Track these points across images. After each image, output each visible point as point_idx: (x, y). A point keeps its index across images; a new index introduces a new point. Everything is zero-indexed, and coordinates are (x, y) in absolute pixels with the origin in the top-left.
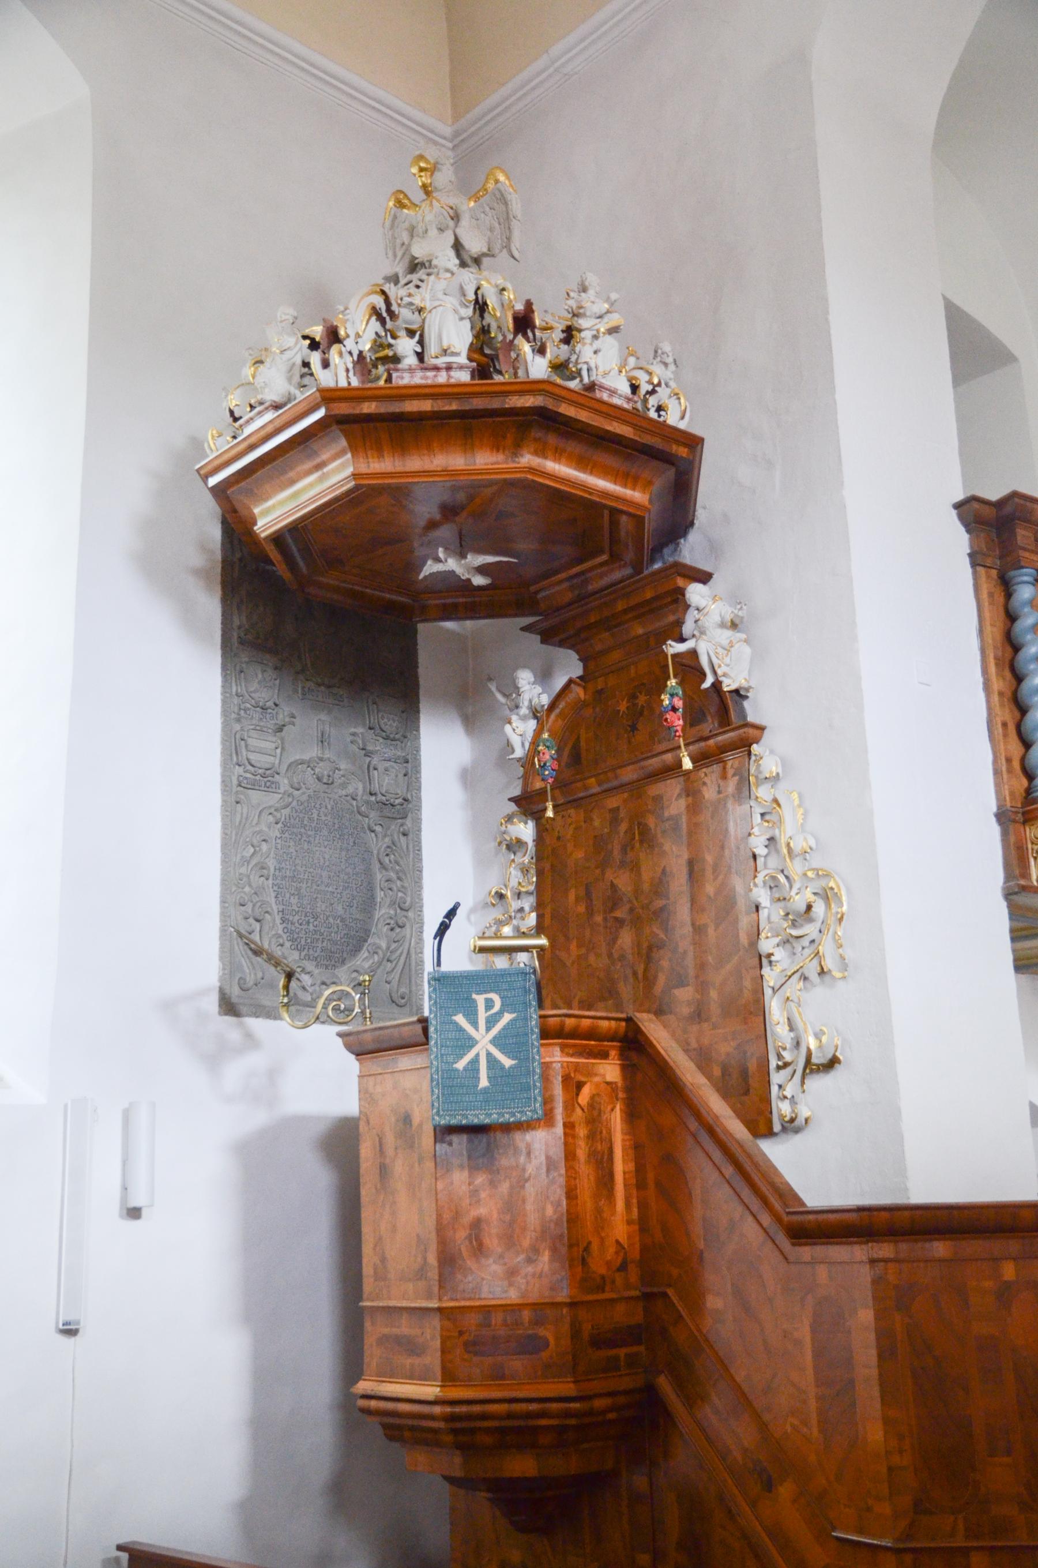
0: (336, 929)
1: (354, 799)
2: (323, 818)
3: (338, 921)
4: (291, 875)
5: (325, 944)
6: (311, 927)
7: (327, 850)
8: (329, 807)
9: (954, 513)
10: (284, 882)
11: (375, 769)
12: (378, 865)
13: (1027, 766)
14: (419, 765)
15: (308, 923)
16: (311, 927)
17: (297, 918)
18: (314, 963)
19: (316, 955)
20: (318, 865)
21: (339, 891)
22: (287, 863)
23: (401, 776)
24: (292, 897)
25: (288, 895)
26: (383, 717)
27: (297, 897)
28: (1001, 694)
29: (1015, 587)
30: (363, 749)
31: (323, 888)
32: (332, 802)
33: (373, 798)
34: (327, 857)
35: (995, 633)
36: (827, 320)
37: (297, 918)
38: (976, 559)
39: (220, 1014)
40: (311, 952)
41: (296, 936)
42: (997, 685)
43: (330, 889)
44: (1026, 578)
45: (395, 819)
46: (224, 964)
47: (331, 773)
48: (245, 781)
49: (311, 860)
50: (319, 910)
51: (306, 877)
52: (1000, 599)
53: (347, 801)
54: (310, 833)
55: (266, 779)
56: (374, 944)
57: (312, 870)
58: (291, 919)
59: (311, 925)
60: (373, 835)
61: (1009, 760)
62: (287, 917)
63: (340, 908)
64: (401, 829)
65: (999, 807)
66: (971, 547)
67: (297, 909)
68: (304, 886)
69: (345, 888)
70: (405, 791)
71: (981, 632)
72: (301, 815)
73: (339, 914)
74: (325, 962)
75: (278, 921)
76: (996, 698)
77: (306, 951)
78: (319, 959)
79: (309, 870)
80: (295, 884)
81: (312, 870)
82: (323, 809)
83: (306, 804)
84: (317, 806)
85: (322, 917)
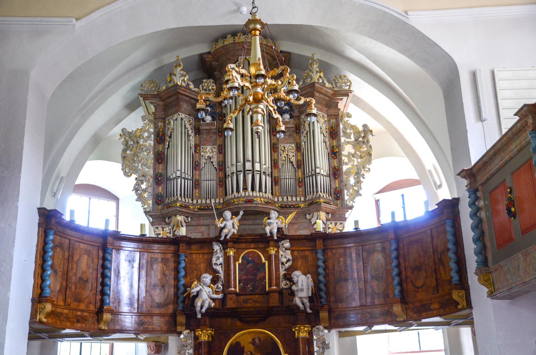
9: (37, 210)
13: (42, 286)
28: (39, 265)
29: (49, 235)
35: (40, 247)
36: (22, 152)
38: (40, 225)
42: (38, 262)
44: (51, 233)
52: (43, 237)
61: (38, 284)
65: (33, 298)
66: (39, 220)
71: (37, 246)
76: (38, 265)
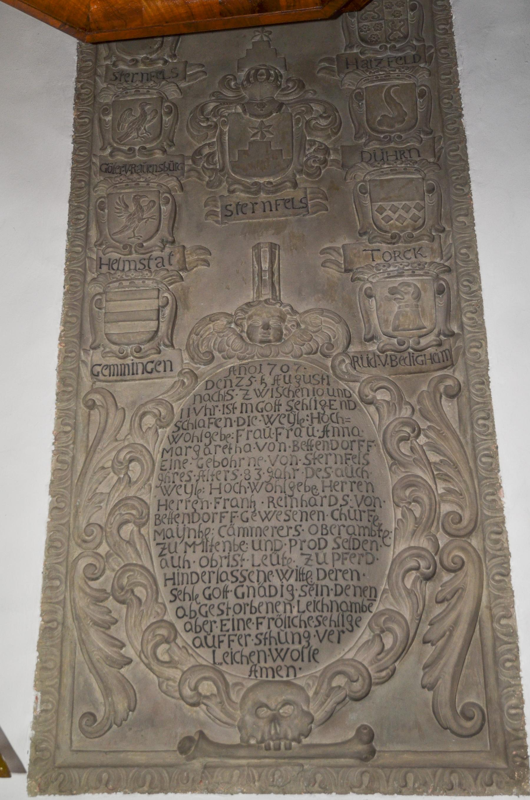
0: (287, 596)
1: (326, 356)
2: (255, 400)
3: (292, 581)
4: (190, 510)
5: (263, 629)
6: (232, 599)
7: (265, 453)
8: (269, 380)
10: (174, 526)
11: (370, 297)
12: (387, 460)
14: (477, 268)
15: (225, 592)
16: (232, 599)
17: (199, 588)
18: (246, 668)
19: (246, 651)
20: (245, 483)
21: (292, 523)
22: (181, 491)
23: (428, 297)
24: (190, 550)
25: (181, 548)
26: (381, 210)
27: (199, 549)
30: (347, 271)
31: (257, 523)
32: (277, 371)
33: (373, 348)
34: (265, 466)
37: (199, 588)
39: (31, 792)
40: (235, 646)
41: (201, 620)
43: (274, 522)
45: (428, 371)
46: (44, 693)
47: (272, 322)
48: (106, 372)
49: (230, 476)
50: (247, 565)
51: (220, 509)
53: (312, 361)
54: (227, 431)
55: (145, 360)
56: (381, 614)
57: (232, 495)
58: (189, 589)
59: (231, 595)
60: (372, 408)
62: (181, 587)
63: (295, 555)
64: (442, 388)
67: (199, 571)
68: (217, 525)
69: (306, 516)
70: (441, 318)
72: (210, 405)
73: (293, 566)
74: (270, 663)
75: (165, 595)
77: (224, 646)
78: (254, 659)
79: (224, 496)
80: (196, 526)
81: (232, 495)
82: (256, 385)
83: (221, 385)
84: (245, 382)
85: (254, 578)
